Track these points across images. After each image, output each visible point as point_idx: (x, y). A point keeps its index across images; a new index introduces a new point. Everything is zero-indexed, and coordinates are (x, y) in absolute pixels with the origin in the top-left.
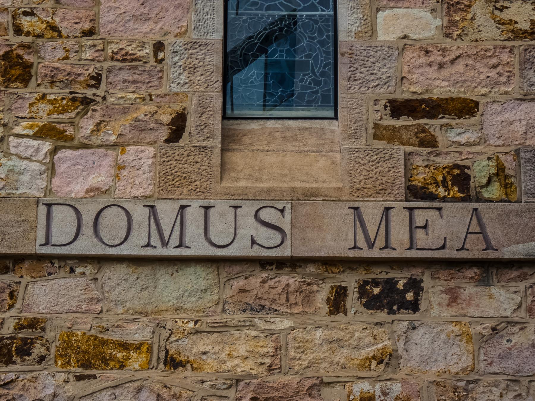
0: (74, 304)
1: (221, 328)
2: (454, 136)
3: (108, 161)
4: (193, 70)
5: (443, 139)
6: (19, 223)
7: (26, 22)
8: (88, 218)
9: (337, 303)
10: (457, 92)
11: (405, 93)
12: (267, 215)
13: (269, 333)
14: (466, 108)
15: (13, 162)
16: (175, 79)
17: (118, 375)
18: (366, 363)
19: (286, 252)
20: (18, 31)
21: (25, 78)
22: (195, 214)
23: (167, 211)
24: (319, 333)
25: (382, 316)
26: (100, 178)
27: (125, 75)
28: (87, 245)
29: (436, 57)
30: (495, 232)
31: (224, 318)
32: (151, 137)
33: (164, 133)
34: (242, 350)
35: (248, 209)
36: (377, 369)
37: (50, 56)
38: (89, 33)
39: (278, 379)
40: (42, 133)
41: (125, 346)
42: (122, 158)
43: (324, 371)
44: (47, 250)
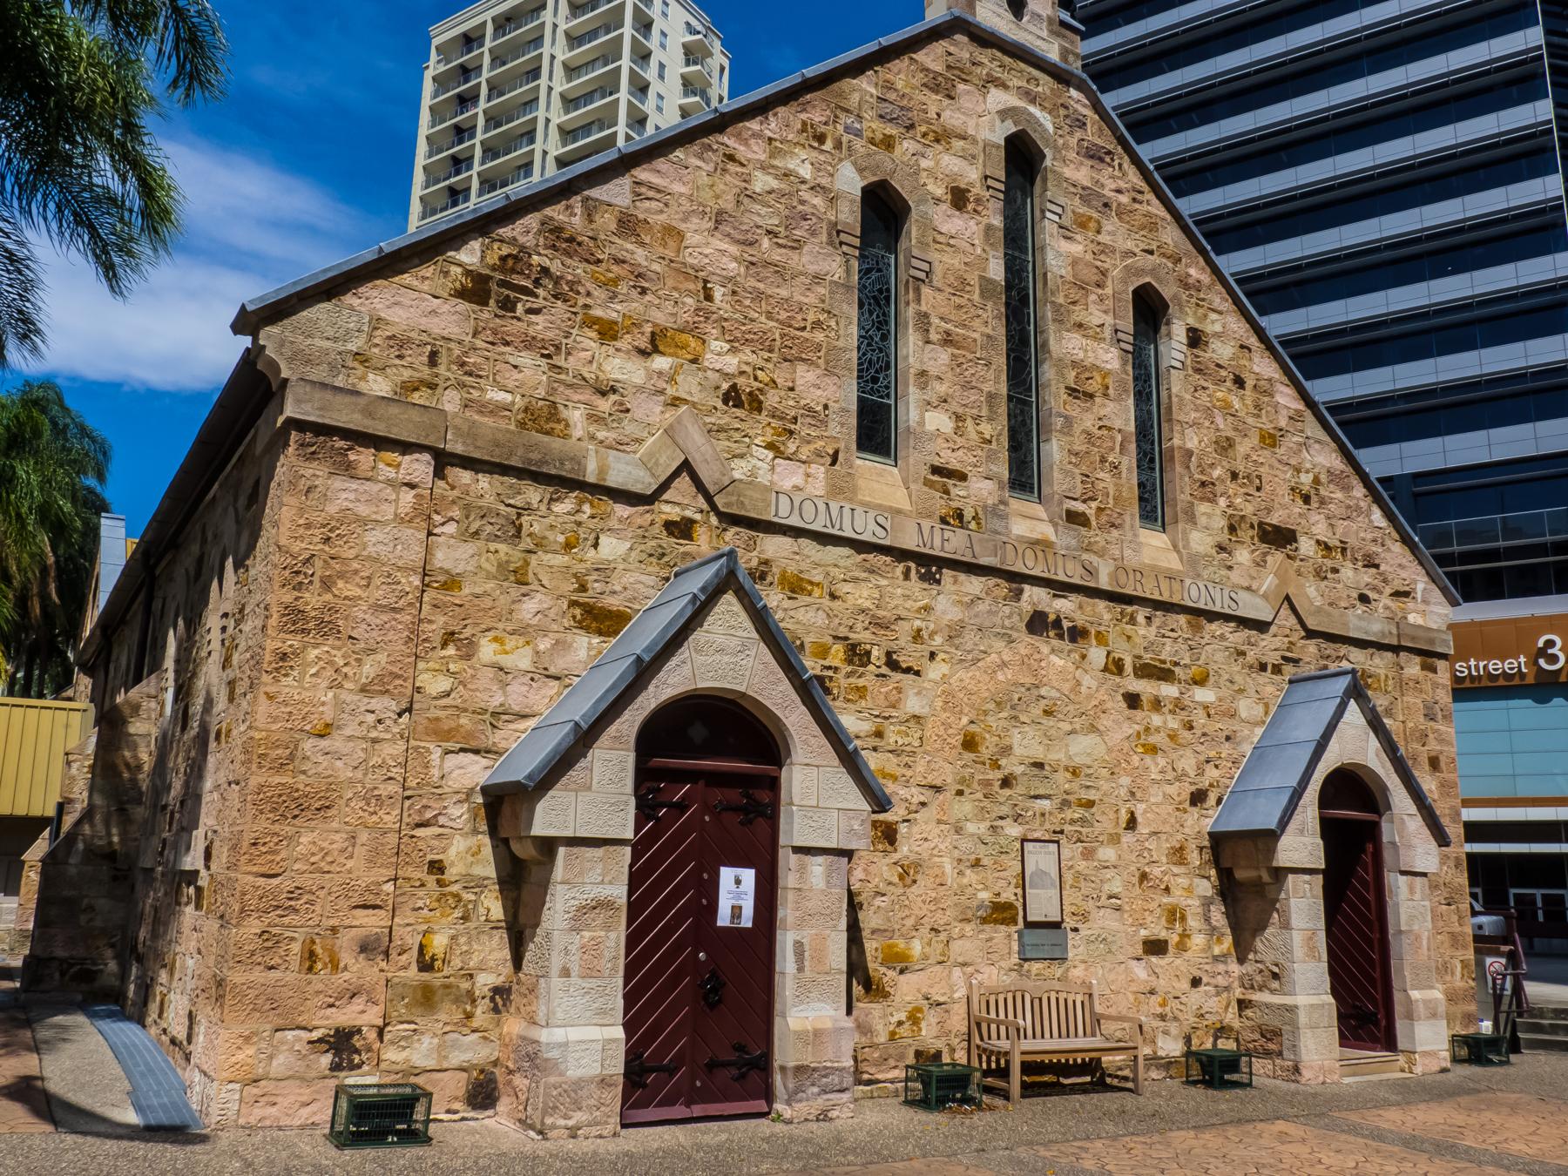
0: (785, 554)
1: (855, 580)
2: (958, 490)
3: (801, 471)
4: (842, 425)
5: (954, 491)
6: (764, 500)
7: (759, 373)
8: (796, 504)
9: (907, 576)
10: (958, 467)
11: (937, 462)
12: (880, 519)
13: (878, 587)
14: (963, 477)
15: (754, 461)
16: (834, 429)
17: (808, 599)
18: (919, 610)
19: (887, 542)
20: (756, 379)
21: (760, 410)
22: (847, 511)
23: (834, 507)
24: (899, 591)
25: (926, 585)
26: (798, 480)
27: (809, 420)
28: (794, 521)
29: (951, 445)
30: (977, 549)
31: (857, 574)
32: (822, 461)
33: (829, 460)
34: (865, 594)
35: (872, 514)
36: (924, 614)
37: (771, 399)
38: (792, 389)
39: (881, 613)
40: (770, 446)
41: (811, 583)
42: (811, 471)
43: (904, 614)
44: (776, 520)
